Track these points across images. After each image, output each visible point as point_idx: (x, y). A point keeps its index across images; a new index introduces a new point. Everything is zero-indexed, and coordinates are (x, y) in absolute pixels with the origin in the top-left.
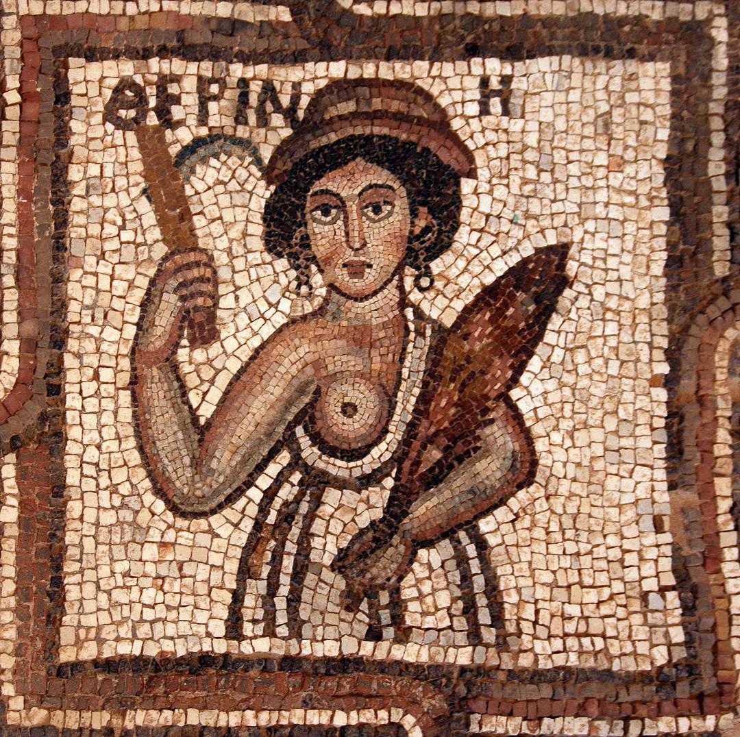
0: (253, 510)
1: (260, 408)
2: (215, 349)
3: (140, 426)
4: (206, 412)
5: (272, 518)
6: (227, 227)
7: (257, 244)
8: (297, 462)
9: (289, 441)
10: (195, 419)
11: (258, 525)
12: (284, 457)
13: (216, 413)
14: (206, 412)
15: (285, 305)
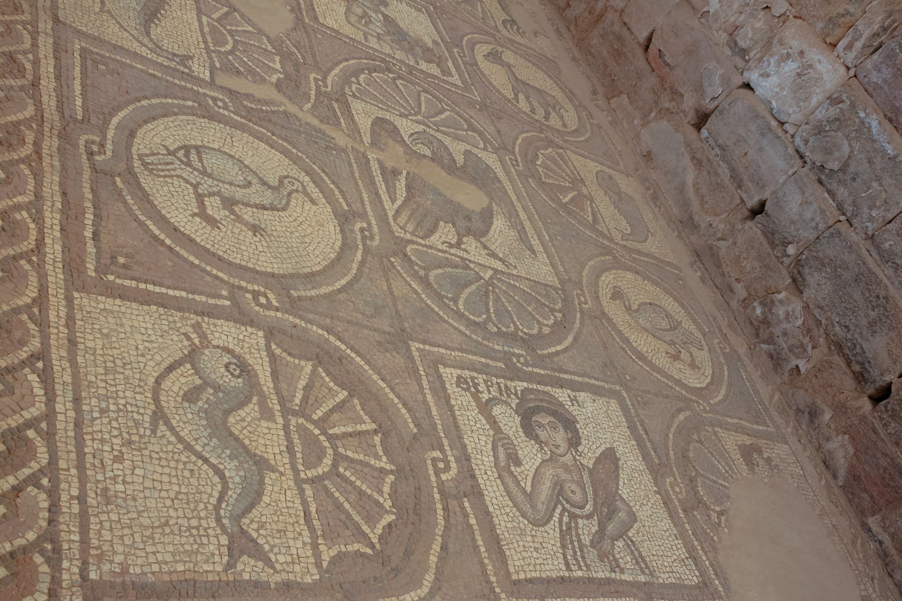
0: (557, 525)
1: (545, 490)
2: (522, 468)
3: (509, 493)
4: (529, 489)
5: (564, 528)
6: (511, 428)
7: (522, 434)
8: (564, 509)
9: (559, 502)
10: (526, 492)
11: (561, 530)
12: (560, 507)
13: (532, 490)
14: (529, 489)
15: (539, 455)
